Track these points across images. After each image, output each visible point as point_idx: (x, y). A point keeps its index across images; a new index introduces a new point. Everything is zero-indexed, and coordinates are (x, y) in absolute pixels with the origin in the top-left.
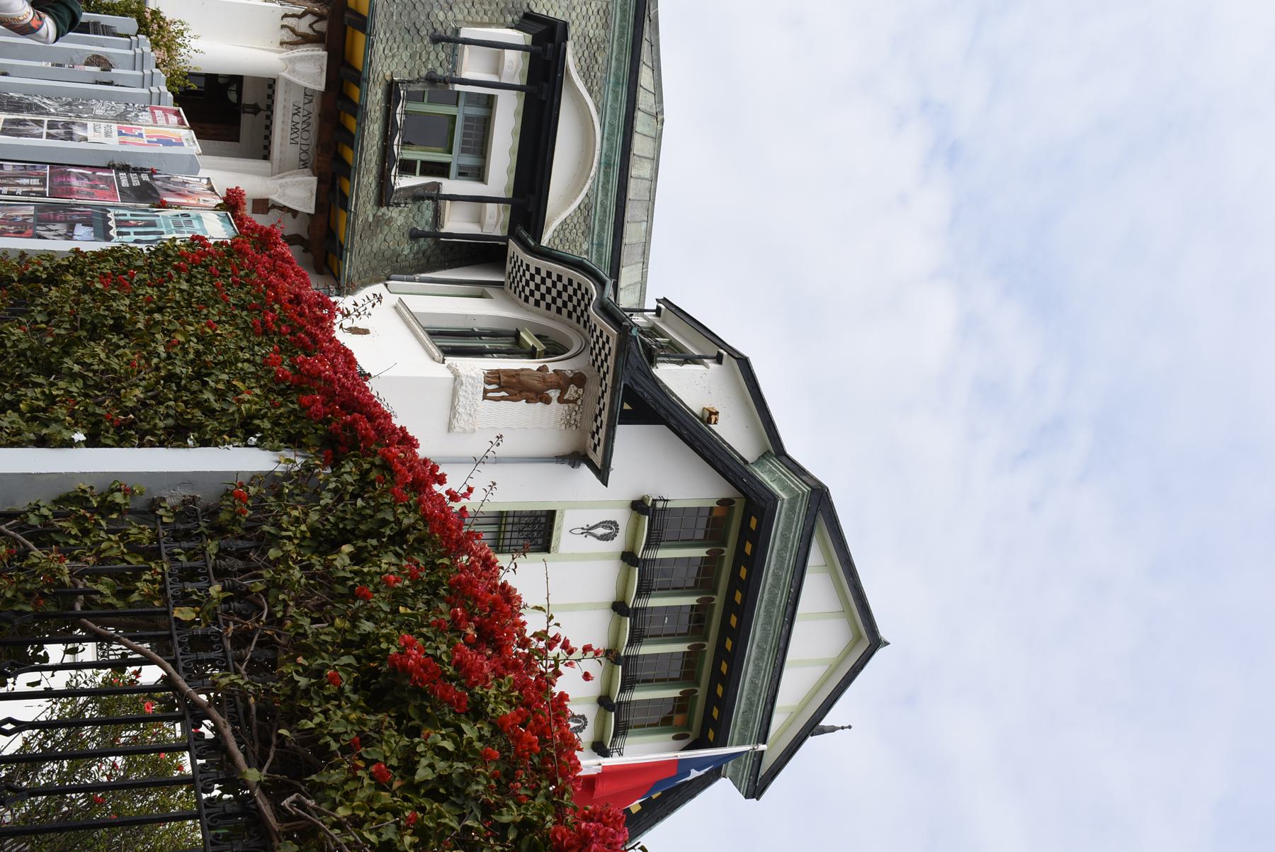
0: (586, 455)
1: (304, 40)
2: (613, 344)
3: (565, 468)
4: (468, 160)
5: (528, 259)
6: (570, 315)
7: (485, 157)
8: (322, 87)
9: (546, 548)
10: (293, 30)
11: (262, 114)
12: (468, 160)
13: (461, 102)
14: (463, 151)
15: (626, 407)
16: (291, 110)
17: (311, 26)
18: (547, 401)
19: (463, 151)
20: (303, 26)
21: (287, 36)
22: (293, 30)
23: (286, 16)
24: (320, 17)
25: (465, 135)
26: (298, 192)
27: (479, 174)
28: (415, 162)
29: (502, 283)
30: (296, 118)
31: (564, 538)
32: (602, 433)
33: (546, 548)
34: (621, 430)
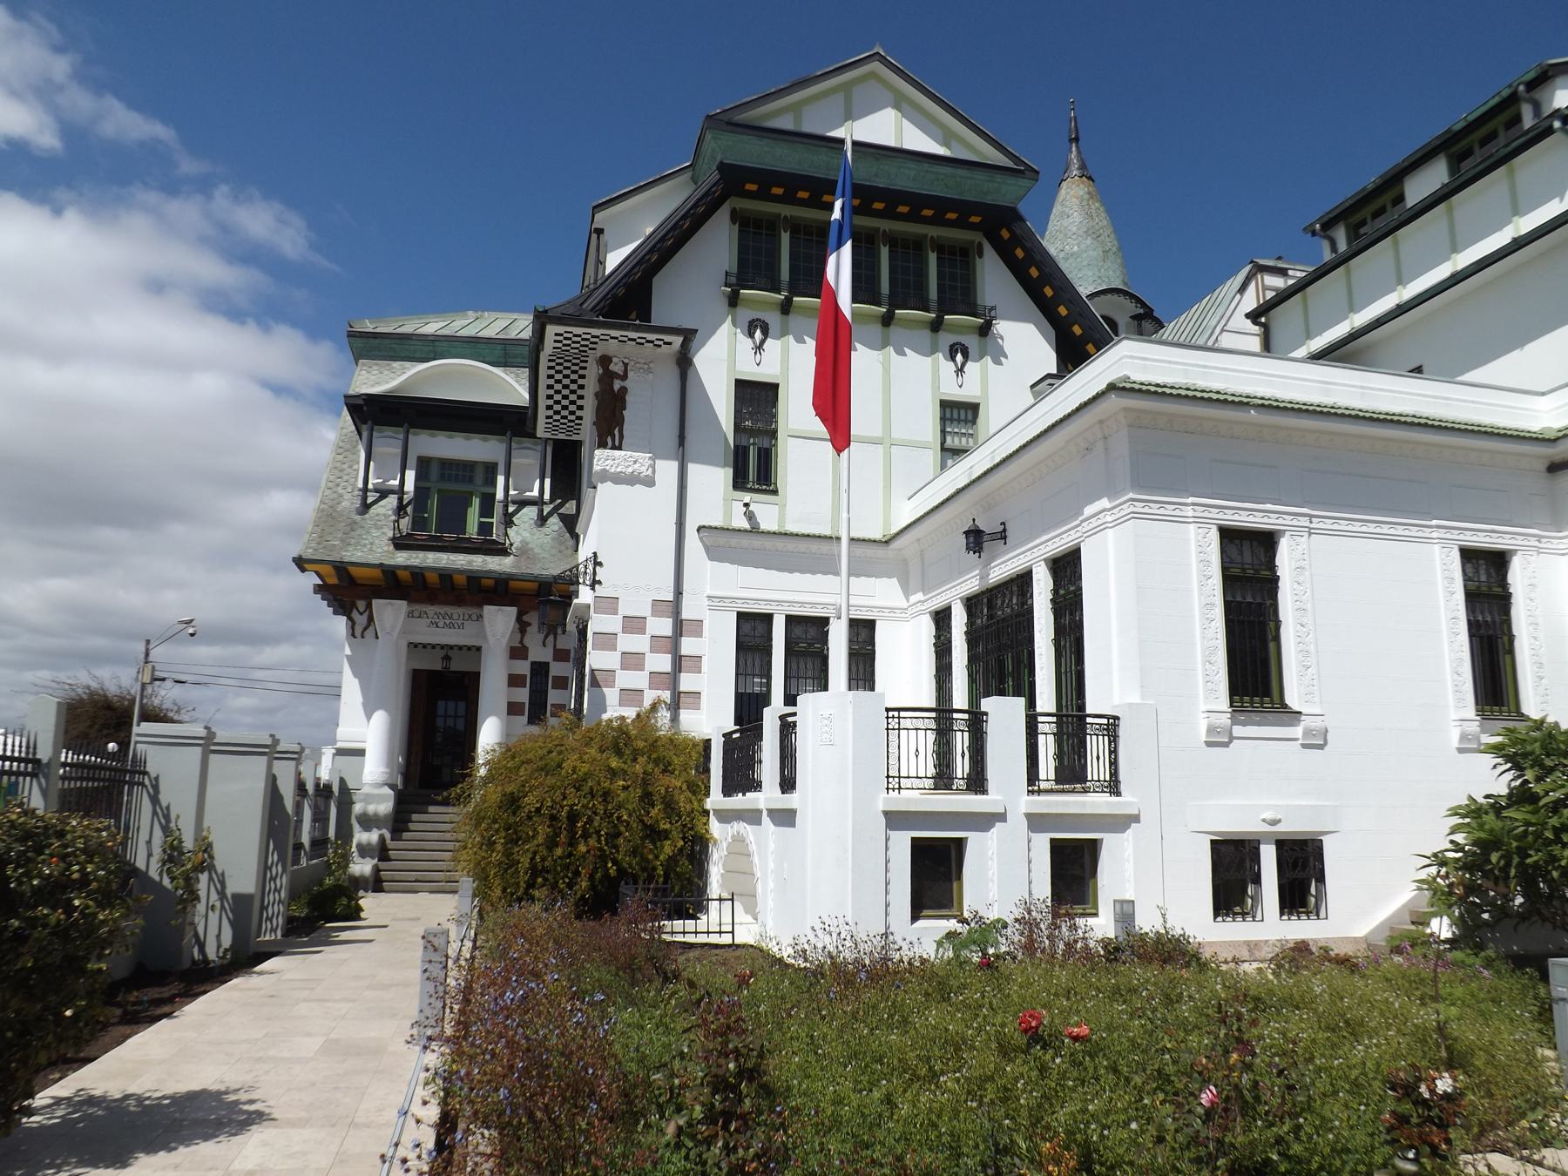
2: (561, 329)
4: (479, 476)
6: (583, 377)
8: (404, 603)
9: (775, 387)
11: (450, 653)
12: (479, 476)
13: (427, 485)
15: (633, 315)
16: (433, 629)
18: (624, 390)
21: (370, 633)
23: (353, 635)
26: (499, 622)
28: (481, 524)
30: (441, 624)
33: (775, 387)
34: (656, 321)
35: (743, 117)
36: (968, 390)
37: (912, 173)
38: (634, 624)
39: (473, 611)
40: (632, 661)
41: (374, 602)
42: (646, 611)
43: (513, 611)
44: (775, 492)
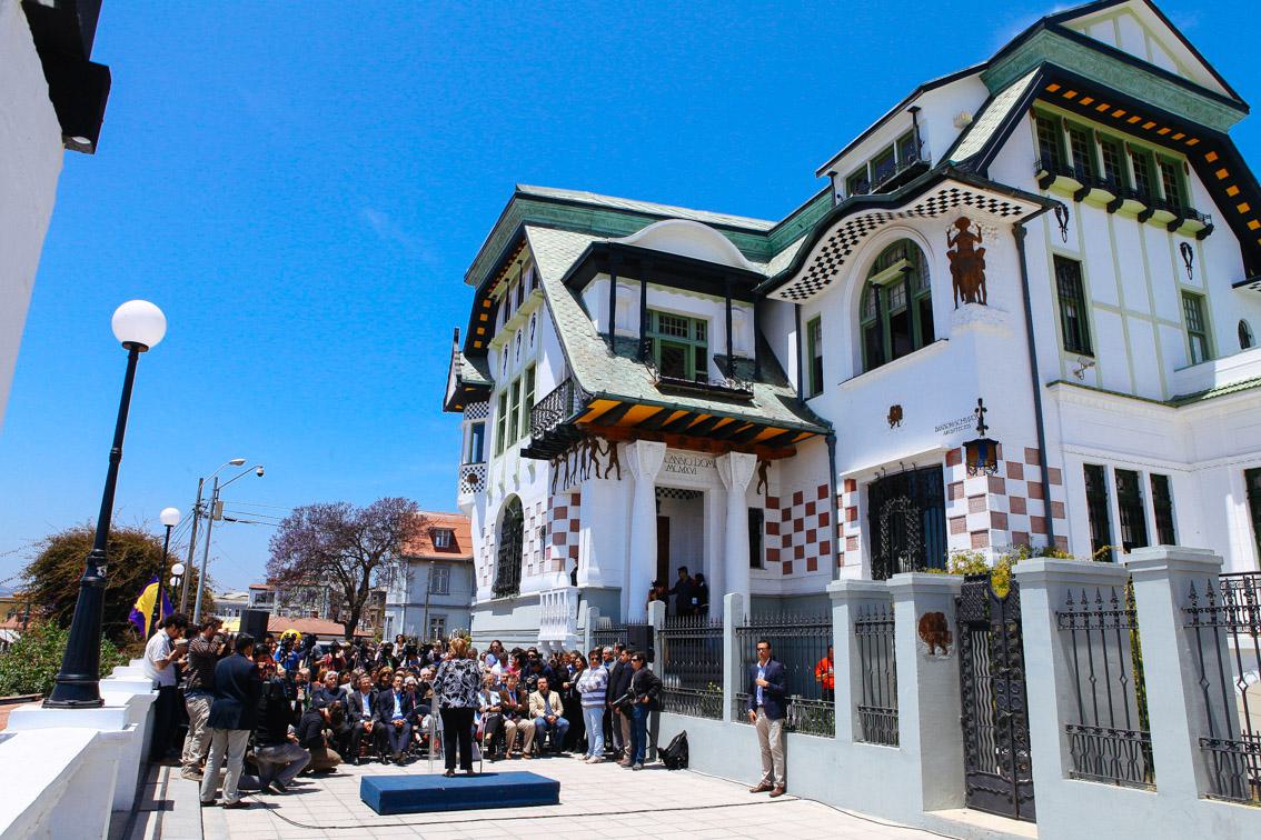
0: (1015, 224)
1: (614, 460)
3: (1026, 239)
4: (693, 331)
5: (798, 279)
7: (689, 318)
8: (664, 445)
9: (1076, 264)
10: (608, 470)
14: (685, 335)
17: (604, 455)
18: (982, 251)
19: (685, 335)
20: (604, 461)
22: (608, 470)
23: (598, 475)
24: (596, 446)
25: (673, 333)
26: (742, 466)
27: (702, 325)
29: (798, 307)
30: (677, 468)
31: (1070, 250)
32: (1013, 202)
33: (1076, 264)
35: (1068, 24)
36: (1195, 286)
37: (1171, 94)
38: (1015, 471)
39: (704, 457)
40: (1018, 506)
41: (619, 445)
42: (1020, 458)
43: (754, 457)
44: (1092, 355)
